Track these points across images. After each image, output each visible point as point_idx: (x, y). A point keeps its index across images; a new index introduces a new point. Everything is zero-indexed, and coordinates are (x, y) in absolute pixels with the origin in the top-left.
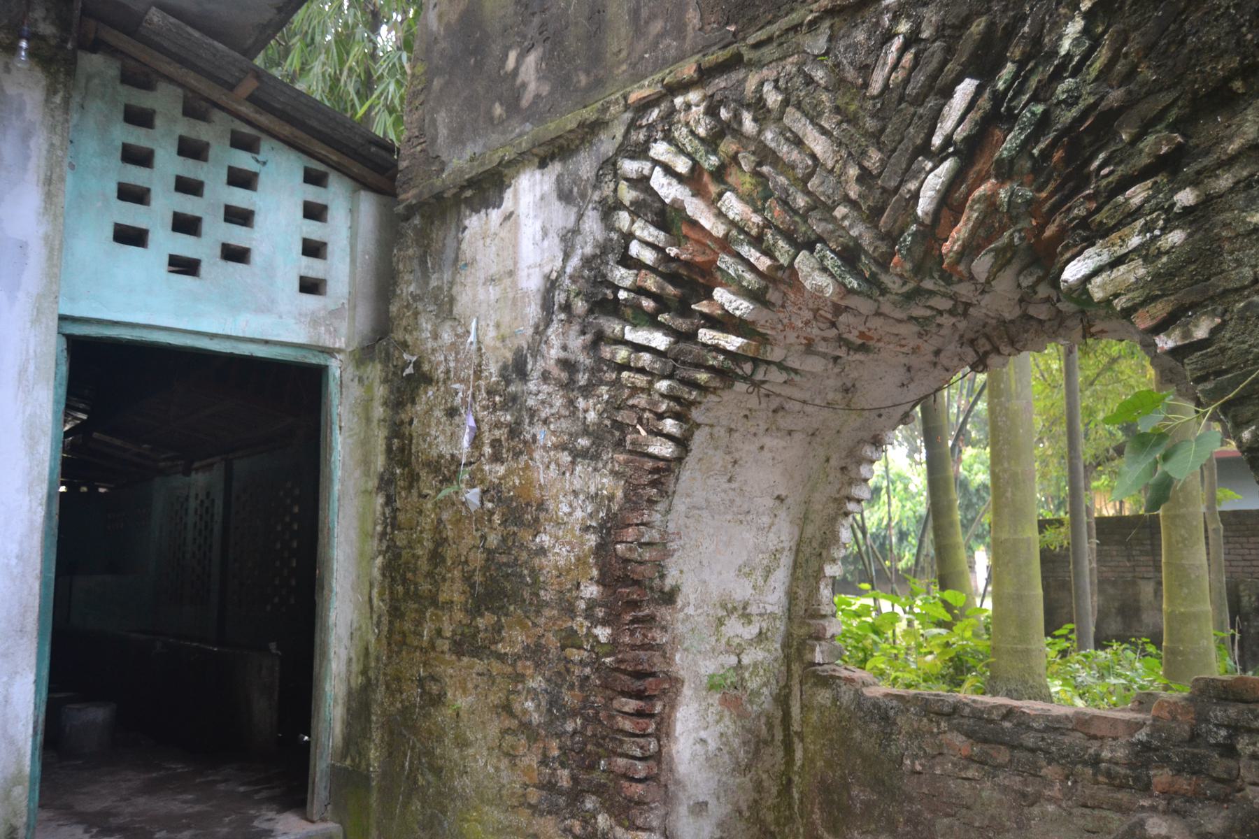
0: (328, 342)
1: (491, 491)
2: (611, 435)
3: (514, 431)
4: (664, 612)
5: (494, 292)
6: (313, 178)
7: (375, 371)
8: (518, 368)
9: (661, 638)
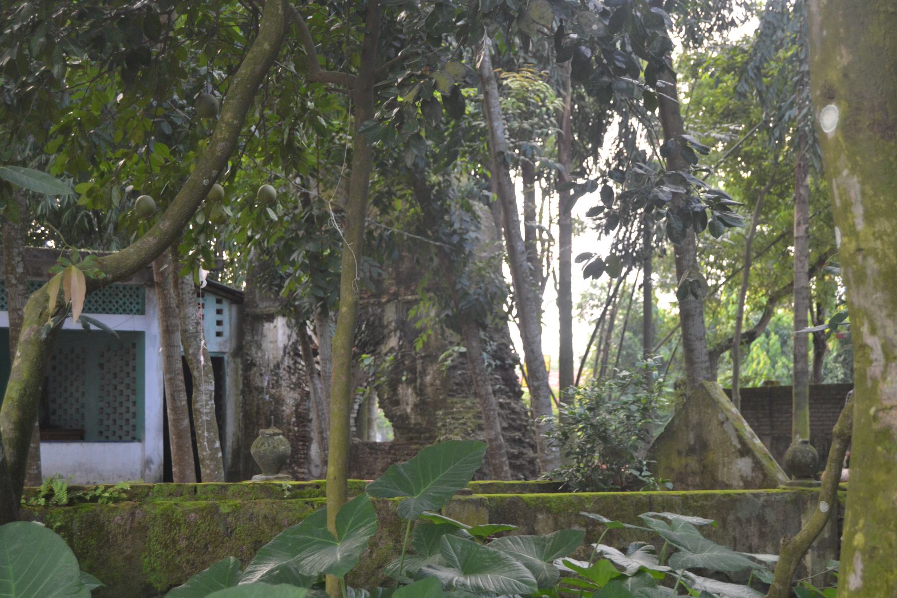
0: (224, 350)
1: (272, 396)
2: (297, 385)
3: (277, 381)
4: (309, 424)
5: (272, 346)
6: (219, 302)
7: (239, 360)
8: (277, 366)
9: (307, 429)
